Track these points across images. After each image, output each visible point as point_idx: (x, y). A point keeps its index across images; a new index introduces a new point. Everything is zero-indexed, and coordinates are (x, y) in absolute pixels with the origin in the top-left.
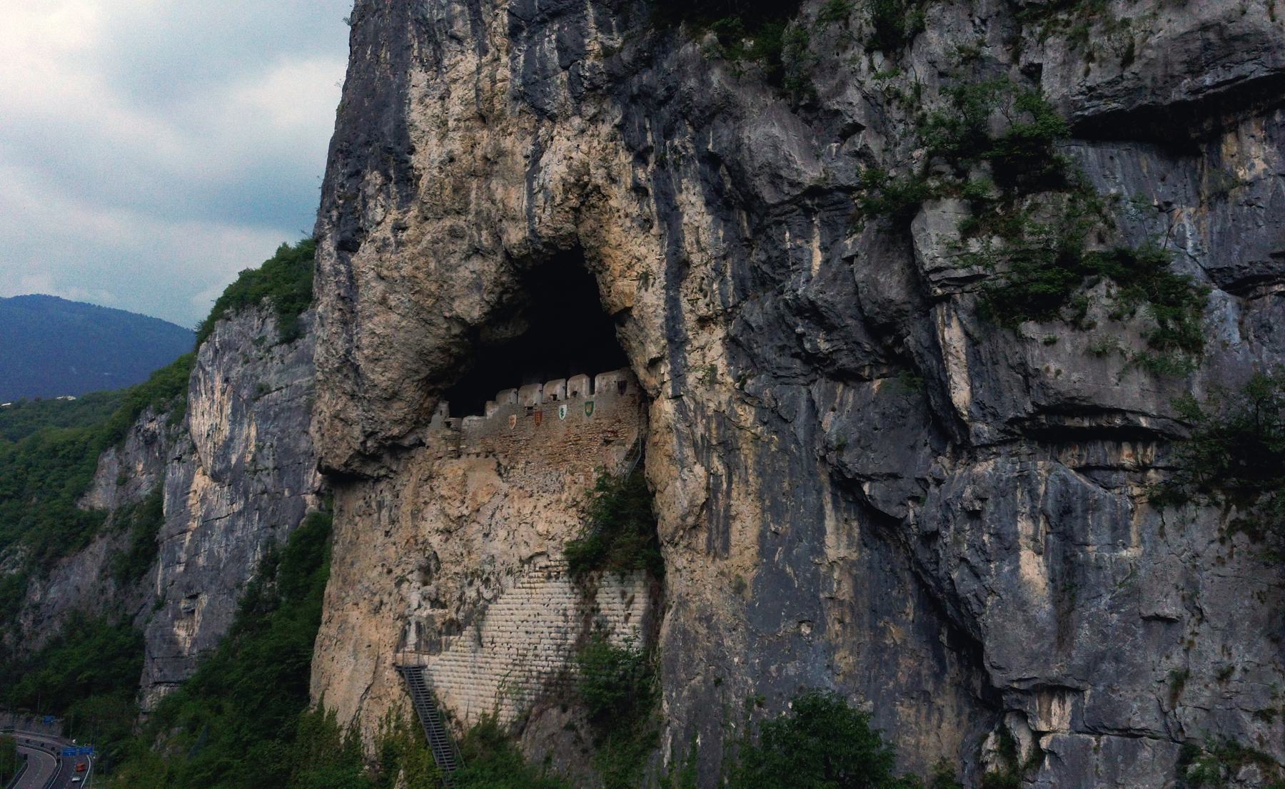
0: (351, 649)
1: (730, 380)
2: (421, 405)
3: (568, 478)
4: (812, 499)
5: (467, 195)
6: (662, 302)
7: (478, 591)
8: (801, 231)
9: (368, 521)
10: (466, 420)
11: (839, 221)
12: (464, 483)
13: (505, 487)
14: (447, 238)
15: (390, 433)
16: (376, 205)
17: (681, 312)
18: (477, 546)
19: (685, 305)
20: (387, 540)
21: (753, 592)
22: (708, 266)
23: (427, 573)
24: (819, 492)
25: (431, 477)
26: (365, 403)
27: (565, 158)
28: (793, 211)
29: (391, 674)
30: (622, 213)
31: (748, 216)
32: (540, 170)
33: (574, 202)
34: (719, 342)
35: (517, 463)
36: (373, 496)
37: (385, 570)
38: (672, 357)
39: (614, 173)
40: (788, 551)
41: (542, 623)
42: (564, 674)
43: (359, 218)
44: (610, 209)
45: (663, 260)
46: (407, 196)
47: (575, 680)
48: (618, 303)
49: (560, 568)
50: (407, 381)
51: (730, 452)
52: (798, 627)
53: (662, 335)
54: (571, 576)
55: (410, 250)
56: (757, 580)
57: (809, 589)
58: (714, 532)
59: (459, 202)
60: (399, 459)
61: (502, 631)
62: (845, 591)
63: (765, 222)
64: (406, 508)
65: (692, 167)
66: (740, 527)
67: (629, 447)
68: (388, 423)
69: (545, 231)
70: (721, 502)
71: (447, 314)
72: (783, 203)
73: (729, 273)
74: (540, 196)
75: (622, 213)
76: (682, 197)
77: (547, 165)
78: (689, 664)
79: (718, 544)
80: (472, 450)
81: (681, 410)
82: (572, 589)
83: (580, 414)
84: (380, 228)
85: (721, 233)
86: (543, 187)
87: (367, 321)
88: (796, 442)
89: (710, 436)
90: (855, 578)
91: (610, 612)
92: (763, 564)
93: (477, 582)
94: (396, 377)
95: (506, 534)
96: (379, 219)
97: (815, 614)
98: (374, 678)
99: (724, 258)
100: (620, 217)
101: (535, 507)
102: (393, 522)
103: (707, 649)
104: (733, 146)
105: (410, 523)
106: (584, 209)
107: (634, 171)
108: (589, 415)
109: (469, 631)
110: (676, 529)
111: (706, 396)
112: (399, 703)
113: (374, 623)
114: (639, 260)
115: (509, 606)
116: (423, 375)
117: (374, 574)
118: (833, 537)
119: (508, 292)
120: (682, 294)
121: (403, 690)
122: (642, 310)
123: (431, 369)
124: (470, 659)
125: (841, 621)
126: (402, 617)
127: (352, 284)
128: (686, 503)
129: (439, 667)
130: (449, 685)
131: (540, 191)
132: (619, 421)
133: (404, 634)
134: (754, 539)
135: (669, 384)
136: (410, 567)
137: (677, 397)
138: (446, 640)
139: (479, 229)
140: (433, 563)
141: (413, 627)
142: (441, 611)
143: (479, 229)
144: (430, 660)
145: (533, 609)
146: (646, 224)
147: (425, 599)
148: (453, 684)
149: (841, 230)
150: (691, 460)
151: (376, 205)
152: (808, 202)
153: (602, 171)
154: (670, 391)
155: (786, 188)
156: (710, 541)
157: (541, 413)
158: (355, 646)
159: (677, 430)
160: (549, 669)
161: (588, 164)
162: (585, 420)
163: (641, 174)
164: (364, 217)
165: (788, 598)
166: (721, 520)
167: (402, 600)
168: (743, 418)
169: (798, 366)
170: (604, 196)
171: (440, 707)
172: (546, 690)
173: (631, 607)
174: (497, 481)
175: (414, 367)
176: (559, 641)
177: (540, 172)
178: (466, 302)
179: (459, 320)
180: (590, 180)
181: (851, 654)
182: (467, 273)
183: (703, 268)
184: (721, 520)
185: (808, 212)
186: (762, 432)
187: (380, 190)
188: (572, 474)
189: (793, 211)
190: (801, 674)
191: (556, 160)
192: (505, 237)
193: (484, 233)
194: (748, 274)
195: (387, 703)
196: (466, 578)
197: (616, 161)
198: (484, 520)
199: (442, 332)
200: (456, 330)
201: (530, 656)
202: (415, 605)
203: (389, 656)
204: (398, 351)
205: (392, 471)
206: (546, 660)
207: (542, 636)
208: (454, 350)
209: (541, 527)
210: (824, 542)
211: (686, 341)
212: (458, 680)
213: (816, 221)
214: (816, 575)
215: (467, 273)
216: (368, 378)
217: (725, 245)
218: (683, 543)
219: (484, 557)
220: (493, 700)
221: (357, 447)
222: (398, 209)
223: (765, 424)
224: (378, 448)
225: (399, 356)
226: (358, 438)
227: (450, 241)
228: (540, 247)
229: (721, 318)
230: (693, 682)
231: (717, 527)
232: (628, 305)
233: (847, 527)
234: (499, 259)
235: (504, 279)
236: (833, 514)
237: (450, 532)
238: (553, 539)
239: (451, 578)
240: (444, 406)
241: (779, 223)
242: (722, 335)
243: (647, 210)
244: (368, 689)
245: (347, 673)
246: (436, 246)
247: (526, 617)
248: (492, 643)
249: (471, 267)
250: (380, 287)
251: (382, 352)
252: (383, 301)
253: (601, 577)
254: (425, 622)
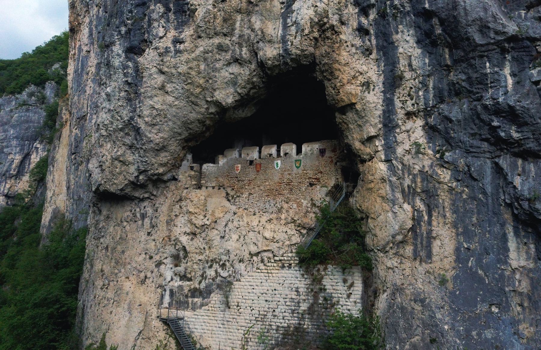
0: (126, 307)
1: (430, 152)
2: (179, 155)
3: (285, 206)
4: (497, 229)
5: (233, 24)
6: (381, 101)
7: (216, 271)
8: (498, 62)
9: (134, 226)
10: (205, 166)
11: (525, 59)
12: (205, 205)
13: (234, 208)
14: (215, 50)
15: (157, 172)
16: (159, 26)
17: (394, 108)
18: (216, 244)
19: (398, 104)
20: (149, 238)
21: (454, 285)
22: (417, 80)
23: (177, 260)
24: (503, 225)
25: (181, 200)
26: (142, 152)
27: (313, 6)
28: (494, 49)
29: (157, 323)
30: (349, 44)
31: (450, 51)
32: (293, 12)
33: (316, 34)
34: (420, 128)
35: (242, 194)
36: (138, 210)
37: (148, 257)
38: (385, 136)
39: (344, 19)
40: (479, 261)
41: (279, 296)
42: (298, 329)
43: (144, 33)
44: (341, 41)
45: (380, 75)
46: (182, 22)
47: (308, 333)
48: (346, 100)
49: (292, 262)
50: (173, 139)
51: (430, 197)
52: (490, 308)
53: (380, 121)
54: (300, 267)
55: (186, 57)
56: (455, 278)
57: (498, 285)
58: (419, 246)
59: (227, 28)
60: (158, 188)
61: (245, 299)
62: (524, 286)
63: (471, 55)
64: (163, 218)
65: (408, 19)
66: (440, 244)
67: (330, 188)
68: (156, 165)
69: (294, 51)
70: (423, 228)
71: (209, 99)
72: (488, 44)
73: (431, 85)
74: (293, 28)
75: (349, 44)
76: (396, 37)
77: (299, 9)
78: (409, 328)
79: (423, 254)
80: (209, 184)
81: (392, 169)
82: (303, 275)
83: (291, 167)
84: (162, 41)
85: (427, 61)
86: (295, 23)
87: (148, 100)
88: (484, 193)
89: (416, 186)
90: (532, 279)
91: (335, 291)
92: (460, 267)
93: (216, 266)
94: (166, 136)
95: (238, 237)
96: (161, 34)
97: (502, 300)
98: (145, 326)
99: (429, 76)
100: (347, 46)
101: (259, 221)
102: (153, 227)
103: (422, 319)
104: (450, 7)
105: (165, 228)
106: (320, 39)
107: (358, 19)
108: (298, 167)
109: (216, 298)
110: (388, 243)
111: (412, 161)
112: (164, 342)
113: (142, 290)
114: (361, 74)
115: (250, 283)
116: (183, 137)
117: (141, 258)
118: (515, 253)
119: (256, 88)
120: (396, 97)
121: (167, 334)
122: (365, 105)
123: (190, 134)
124: (219, 316)
125: (521, 305)
126: (161, 286)
127: (137, 75)
128: (397, 227)
129: (194, 320)
130: (202, 331)
131: (293, 25)
132: (321, 173)
133: (162, 297)
134: (452, 252)
135: (383, 152)
136: (165, 255)
137: (388, 161)
138: (192, 301)
139: (240, 46)
140: (182, 254)
141: (168, 293)
142: (188, 283)
143: (240, 46)
144: (187, 314)
145: (270, 286)
146: (367, 52)
147: (176, 275)
148: (206, 331)
149: (527, 65)
150: (401, 200)
151: (159, 26)
152: (506, 45)
153: (336, 17)
154: (383, 157)
155: (492, 35)
156: (415, 252)
157: (260, 164)
158: (129, 304)
159: (390, 181)
160: (286, 325)
161: (328, 11)
162: (295, 170)
163: (364, 21)
164: (148, 33)
165: (481, 289)
166: (425, 239)
167: (161, 275)
168: (442, 177)
169: (486, 146)
170: (336, 32)
171: (198, 346)
172: (283, 338)
173: (352, 289)
174: (227, 204)
175: (179, 131)
176: (293, 308)
177: (293, 13)
178: (224, 93)
179: (217, 104)
180: (328, 22)
181: (531, 325)
182: (227, 74)
183: (412, 81)
184: (425, 239)
185: (504, 51)
186: (457, 186)
187: (162, 16)
188: (287, 203)
189: (494, 49)
190: (496, 338)
191: (306, 6)
192: (261, 53)
193: (244, 49)
194: (446, 88)
195: (155, 342)
196: (207, 263)
197: (347, 11)
198: (221, 227)
199: (203, 110)
200: (212, 110)
201: (270, 315)
202: (169, 279)
203: (154, 312)
204: (170, 120)
205: (153, 195)
206: (283, 319)
207: (279, 303)
208: (208, 122)
209: (268, 234)
210: (508, 256)
211: (397, 126)
212: (210, 328)
213: (508, 57)
214: (502, 276)
215: (227, 74)
216: (146, 136)
217: (430, 68)
218: (391, 252)
219: (222, 251)
220: (240, 342)
221: (132, 179)
222: (175, 29)
223: (458, 181)
224: (147, 180)
225: (170, 123)
226: (133, 174)
227: (217, 53)
228: (289, 61)
229: (422, 114)
230: (413, 340)
231: (422, 243)
232: (354, 101)
233: (525, 247)
234: (253, 66)
235: (255, 79)
236: (515, 239)
237: (194, 234)
238: (277, 242)
239: (196, 263)
240: (189, 157)
241: (481, 57)
242: (421, 124)
243: (368, 43)
244: (140, 332)
245: (123, 322)
246: (206, 55)
247: (265, 291)
248: (238, 306)
249: (231, 71)
250: (160, 79)
251: (158, 120)
252: (162, 88)
253: (325, 269)
254: (177, 290)
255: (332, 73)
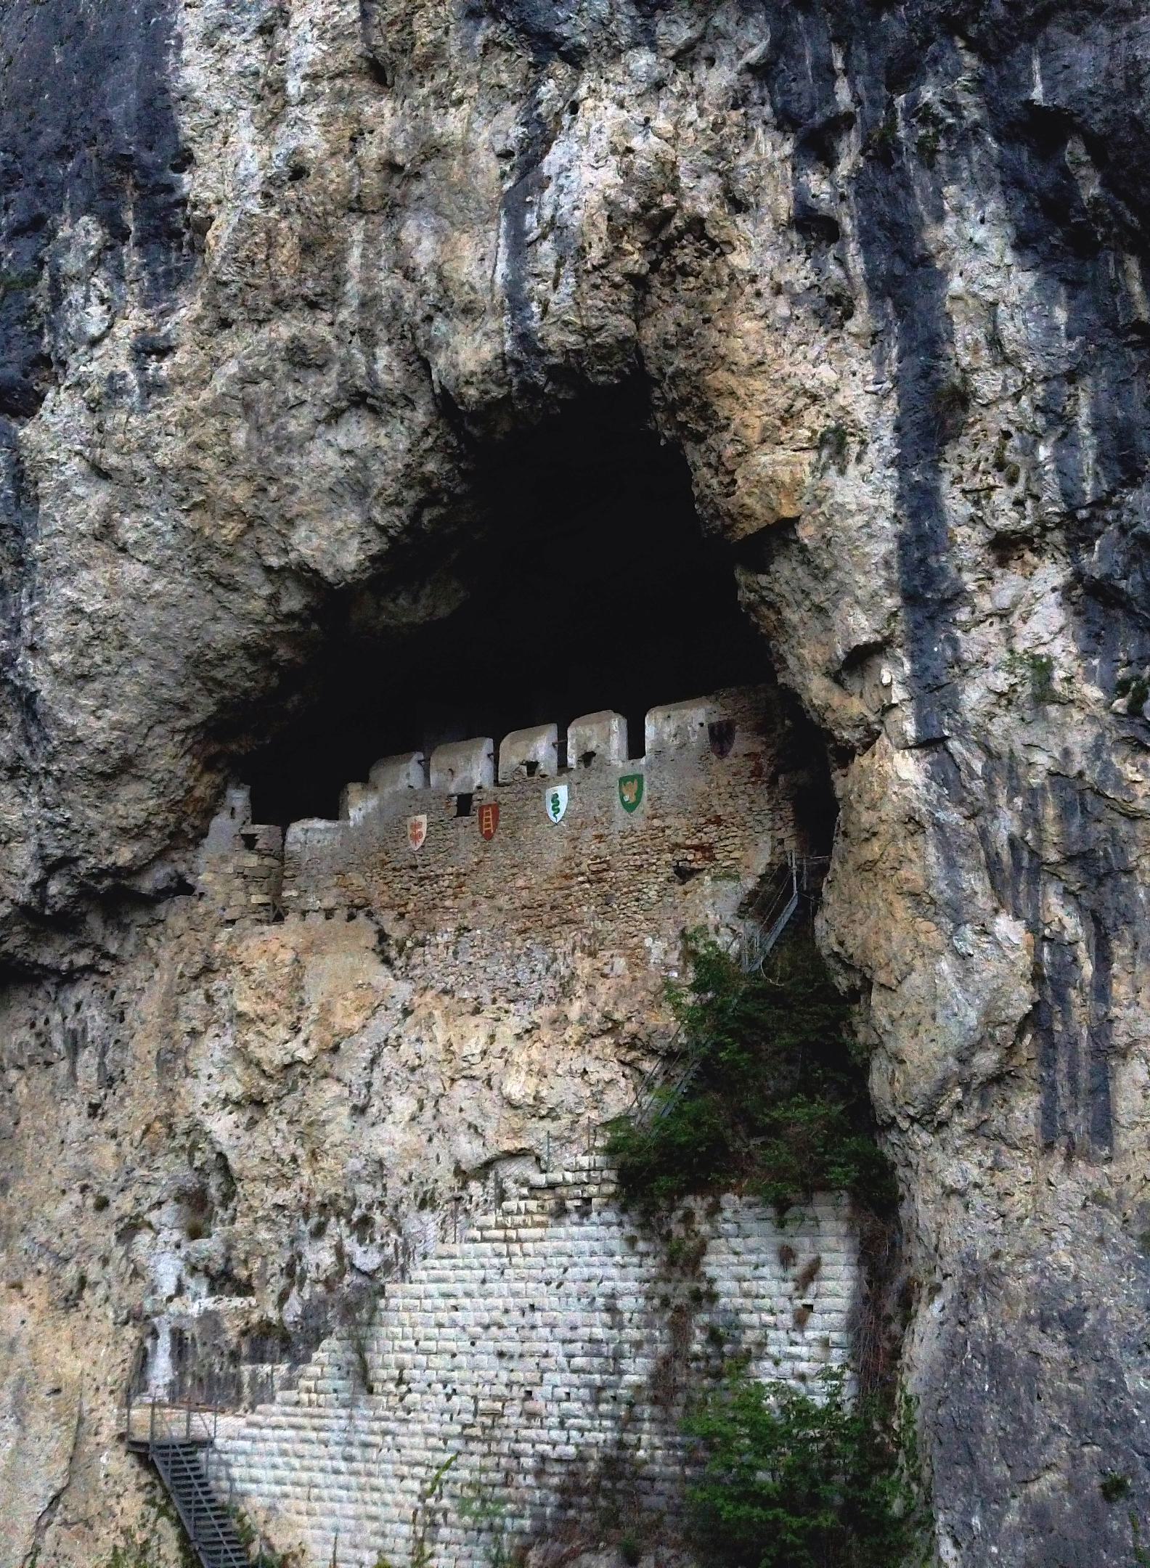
1: (1093, 692)
2: (190, 790)
3: (584, 967)
5: (339, 259)
6: (888, 501)
7: (339, 1251)
9: (42, 1081)
12: (295, 982)
13: (403, 991)
14: (282, 368)
15: (108, 861)
17: (943, 523)
18: (337, 1138)
19: (956, 505)
20: (94, 1125)
22: (1025, 401)
25: (207, 970)
26: (48, 785)
27: (614, 151)
30: (763, 284)
32: (543, 184)
33: (635, 261)
34: (1052, 598)
35: (433, 931)
36: (56, 1017)
37: (90, 1202)
38: (916, 640)
39: (741, 186)
41: (545, 1332)
43: (40, 333)
44: (732, 277)
45: (886, 396)
46: (168, 273)
47: (652, 1479)
48: (758, 508)
49: (593, 1189)
50: (159, 730)
51: (1100, 881)
53: (889, 585)
54: (623, 1210)
58: (1063, 1089)
59: (317, 278)
60: (124, 928)
61: (427, 1353)
64: (145, 1046)
65: (976, 153)
67: (750, 884)
69: (555, 337)
70: (1078, 1014)
71: (274, 561)
73: (1084, 414)
75: (763, 284)
77: (564, 170)
79: (1077, 1122)
80: (312, 901)
82: (632, 1241)
83: (606, 808)
84: (97, 352)
85: (1061, 316)
86: (554, 226)
89: (1040, 840)
91: (748, 1303)
93: (337, 1228)
94: (130, 719)
95: (414, 1106)
96: (94, 330)
98: (71, 1473)
99: (1071, 377)
100: (758, 294)
101: (492, 1037)
102: (109, 1082)
103: (1071, 1398)
104: (1119, 84)
105: (153, 1085)
106: (656, 280)
107: (796, 181)
108: (630, 807)
109: (329, 1352)
110: (942, 1088)
111: (1022, 736)
112: (140, 1537)
113: (65, 1334)
114: (815, 398)
115: (444, 1287)
116: (198, 717)
117: (64, 1209)
119: (438, 502)
120: (947, 478)
122: (829, 522)
123: (222, 704)
124: (335, 1424)
126: (137, 1317)
127: (20, 491)
128: (972, 1017)
129: (247, 1445)
130: (277, 1490)
131: (543, 237)
132: (718, 821)
133: (143, 1360)
135: (908, 710)
136: (155, 1193)
137: (929, 743)
138: (254, 1376)
139: (368, 339)
140: (214, 1185)
141: (165, 1342)
142: (237, 1302)
145: (515, 1294)
147: (194, 1270)
148: (288, 1489)
150: (984, 902)
153: (710, 183)
154: (910, 729)
156: (1048, 1114)
157: (496, 808)
159: (938, 825)
160: (571, 1450)
163: (818, 186)
164: (53, 329)
166: (1084, 1060)
167: (136, 1274)
170: (713, 245)
171: (255, 1549)
172: (563, 1507)
173: (813, 1287)
174: (380, 976)
175: (180, 695)
176: (597, 1378)
177: (543, 188)
178: (325, 530)
179: (304, 575)
180: (679, 206)
182: (331, 457)
183: (1008, 406)
184: (1084, 1060)
187: (98, 262)
188: (593, 954)
191: (588, 156)
193: (383, 352)
195: (108, 1537)
196: (307, 1217)
197: (750, 155)
198: (353, 1070)
199: (257, 606)
200: (293, 602)
201: (513, 1415)
202: (168, 1287)
203: (108, 1417)
204: (141, 654)
205: (106, 956)
206: (562, 1425)
207: (545, 1363)
208: (283, 652)
209: (517, 1087)
211: (959, 596)
212: (305, 1476)
215: (331, 457)
216: (58, 724)
217: (1073, 346)
218: (962, 1122)
219: (355, 1164)
220: (406, 1530)
221: (21, 895)
222: (145, 305)
224: (76, 899)
225: (142, 667)
226: (25, 875)
227: (288, 376)
228: (540, 378)
229: (1057, 537)
230: (1034, 1488)
231: (1072, 1078)
232: (787, 512)
234: (420, 416)
235: (431, 466)
237: (259, 1104)
238: (552, 1115)
239: (263, 1218)
240: (239, 798)
242: (1058, 580)
243: (835, 271)
244: (56, 1499)
246: (251, 389)
247: (497, 1315)
248: (400, 1381)
249: (342, 442)
250: (97, 498)
251: (98, 659)
252: (105, 532)
253: (714, 1210)
254: (196, 1330)
255: (705, 411)
